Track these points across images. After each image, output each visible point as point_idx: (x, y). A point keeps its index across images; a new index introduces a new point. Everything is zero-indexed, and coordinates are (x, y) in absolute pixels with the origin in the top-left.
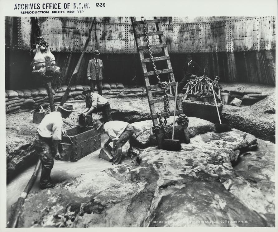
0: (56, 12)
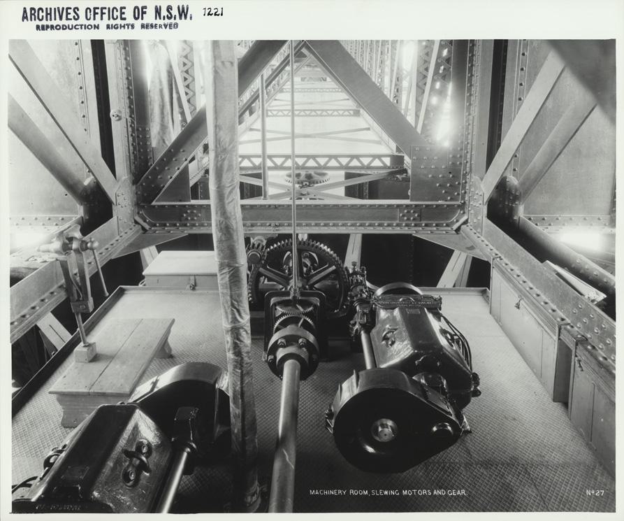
0: (116, 27)
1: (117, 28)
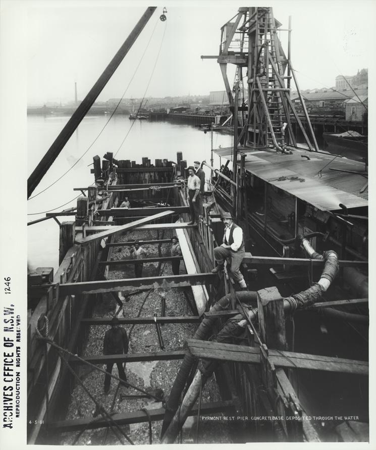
0: (18, 361)
1: (19, 359)
